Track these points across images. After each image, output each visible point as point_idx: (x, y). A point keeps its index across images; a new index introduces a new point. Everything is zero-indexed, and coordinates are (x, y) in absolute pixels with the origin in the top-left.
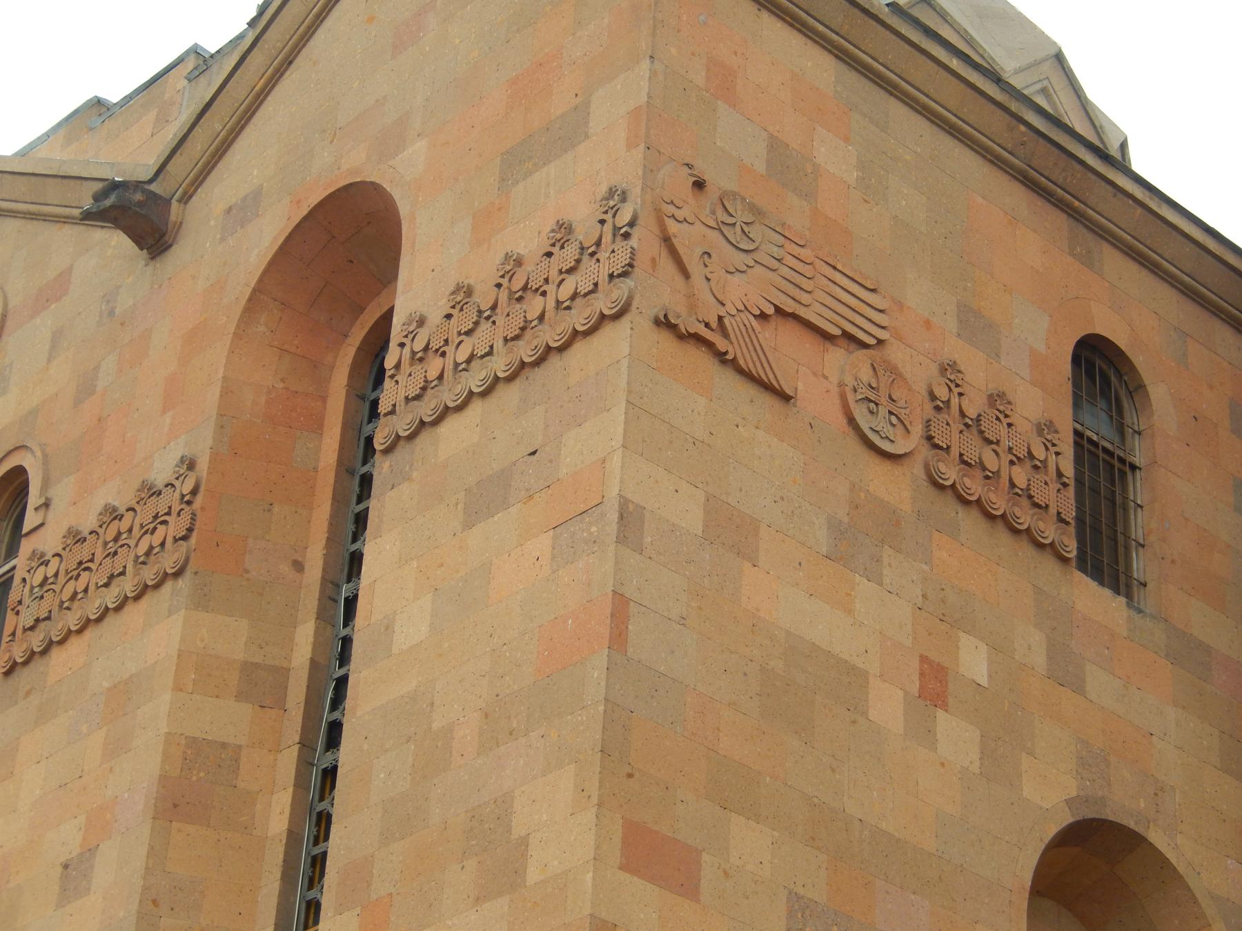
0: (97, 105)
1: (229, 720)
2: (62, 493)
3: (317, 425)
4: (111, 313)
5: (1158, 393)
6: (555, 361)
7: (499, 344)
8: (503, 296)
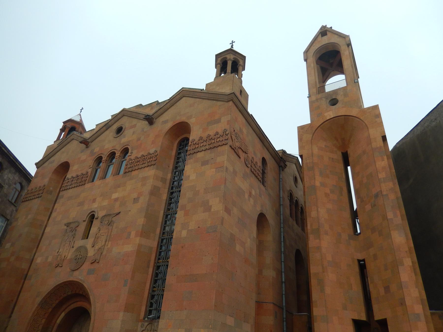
0: (141, 105)
1: (159, 184)
2: (135, 152)
3: (172, 150)
5: (268, 165)
6: (216, 148)
7: (207, 145)
8: (208, 139)
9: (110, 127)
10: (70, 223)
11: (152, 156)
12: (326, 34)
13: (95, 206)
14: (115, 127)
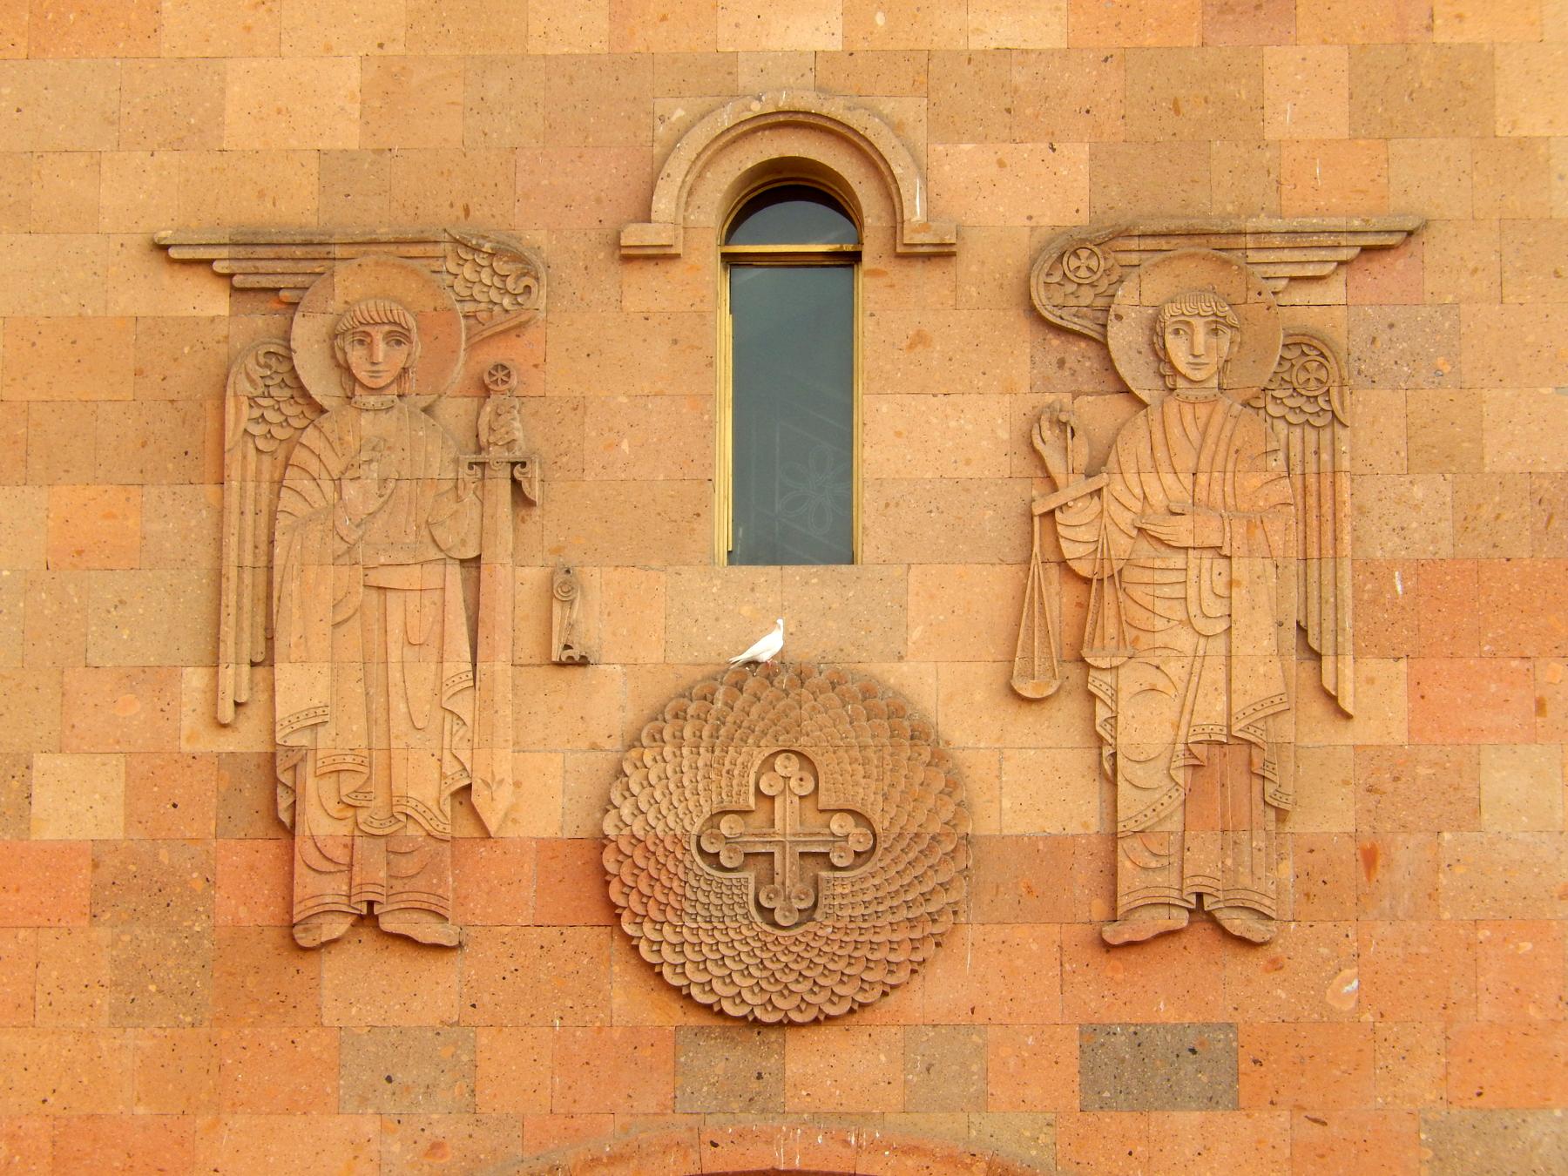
10: (317, 250)
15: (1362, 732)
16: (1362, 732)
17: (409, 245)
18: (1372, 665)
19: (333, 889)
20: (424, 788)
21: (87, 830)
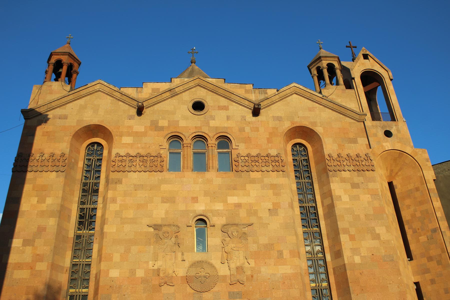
4: (245, 120)
7: (352, 166)
9: (177, 94)
10: (161, 226)
11: (277, 159)
12: (368, 59)
13: (200, 208)
14: (189, 98)
15: (251, 266)
16: (251, 266)
17: (169, 225)
18: (251, 260)
19: (162, 281)
20: (171, 272)
21: (141, 276)
